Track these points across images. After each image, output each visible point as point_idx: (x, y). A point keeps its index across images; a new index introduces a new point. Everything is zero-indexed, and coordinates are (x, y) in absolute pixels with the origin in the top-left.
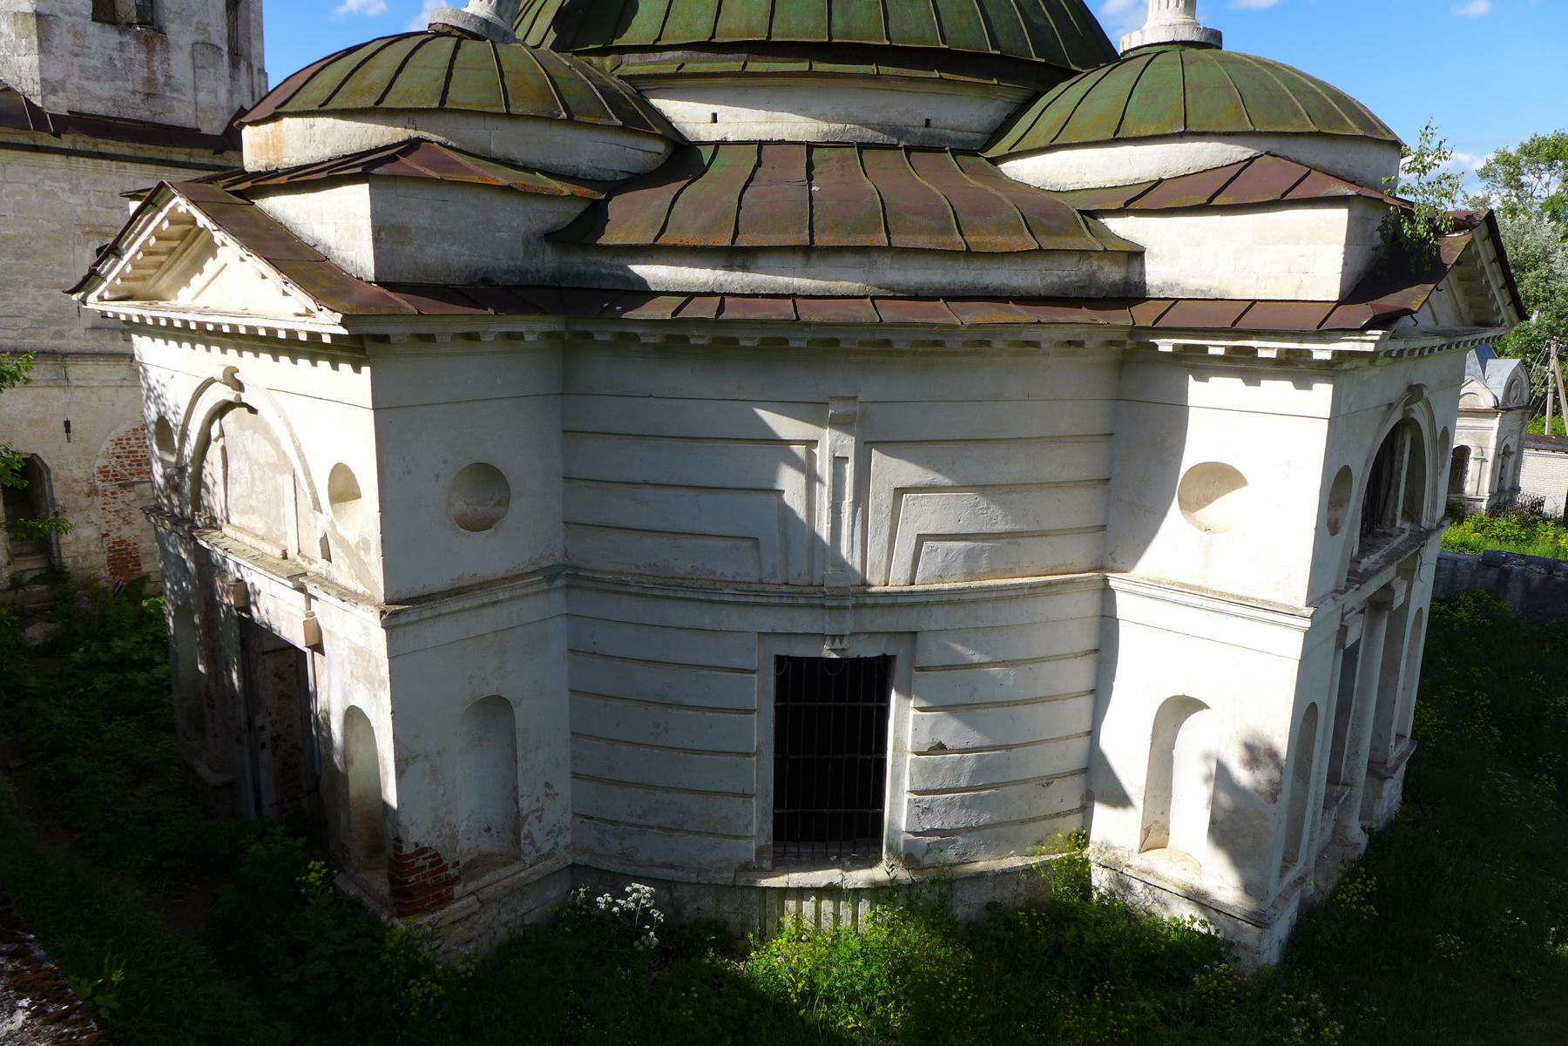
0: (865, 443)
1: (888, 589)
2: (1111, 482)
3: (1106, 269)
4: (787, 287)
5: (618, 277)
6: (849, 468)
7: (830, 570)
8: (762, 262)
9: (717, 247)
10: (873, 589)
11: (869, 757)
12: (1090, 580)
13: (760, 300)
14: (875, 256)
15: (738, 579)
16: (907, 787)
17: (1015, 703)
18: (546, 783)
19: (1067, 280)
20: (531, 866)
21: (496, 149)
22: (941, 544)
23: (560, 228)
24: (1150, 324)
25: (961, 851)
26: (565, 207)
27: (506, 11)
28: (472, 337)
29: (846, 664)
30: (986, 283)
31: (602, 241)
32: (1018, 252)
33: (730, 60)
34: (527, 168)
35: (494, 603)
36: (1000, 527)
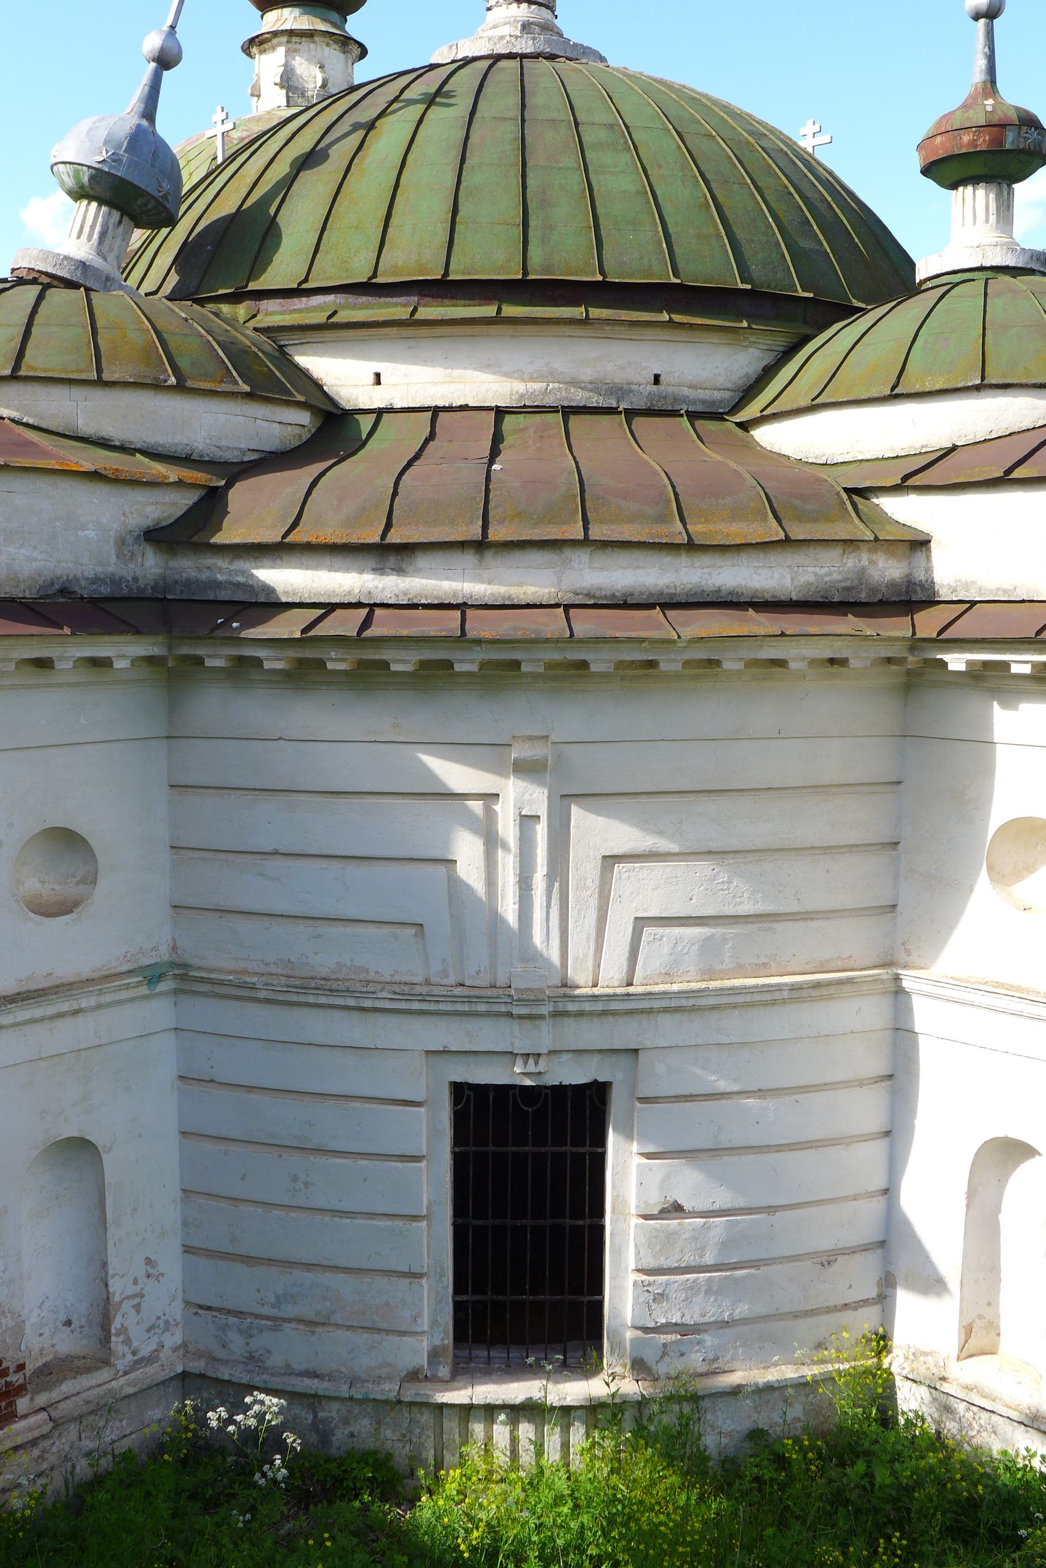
0: (562, 796)
1: (597, 991)
2: (901, 847)
3: (881, 564)
4: (455, 595)
5: (238, 585)
6: (541, 830)
7: (518, 968)
8: (422, 561)
9: (363, 544)
10: (578, 992)
11: (581, 1223)
12: (876, 980)
13: (420, 612)
14: (568, 552)
15: (397, 978)
16: (632, 1265)
17: (779, 1148)
18: (147, 1258)
19: (827, 579)
20: (126, 1373)
21: (85, 426)
22: (667, 931)
23: (164, 524)
24: (934, 635)
25: (711, 1356)
26: (172, 496)
27: (111, 250)
28: (43, 664)
29: (546, 1094)
30: (717, 585)
31: (218, 539)
32: (757, 544)
33: (396, 305)
34: (122, 448)
35: (76, 1012)
36: (747, 908)
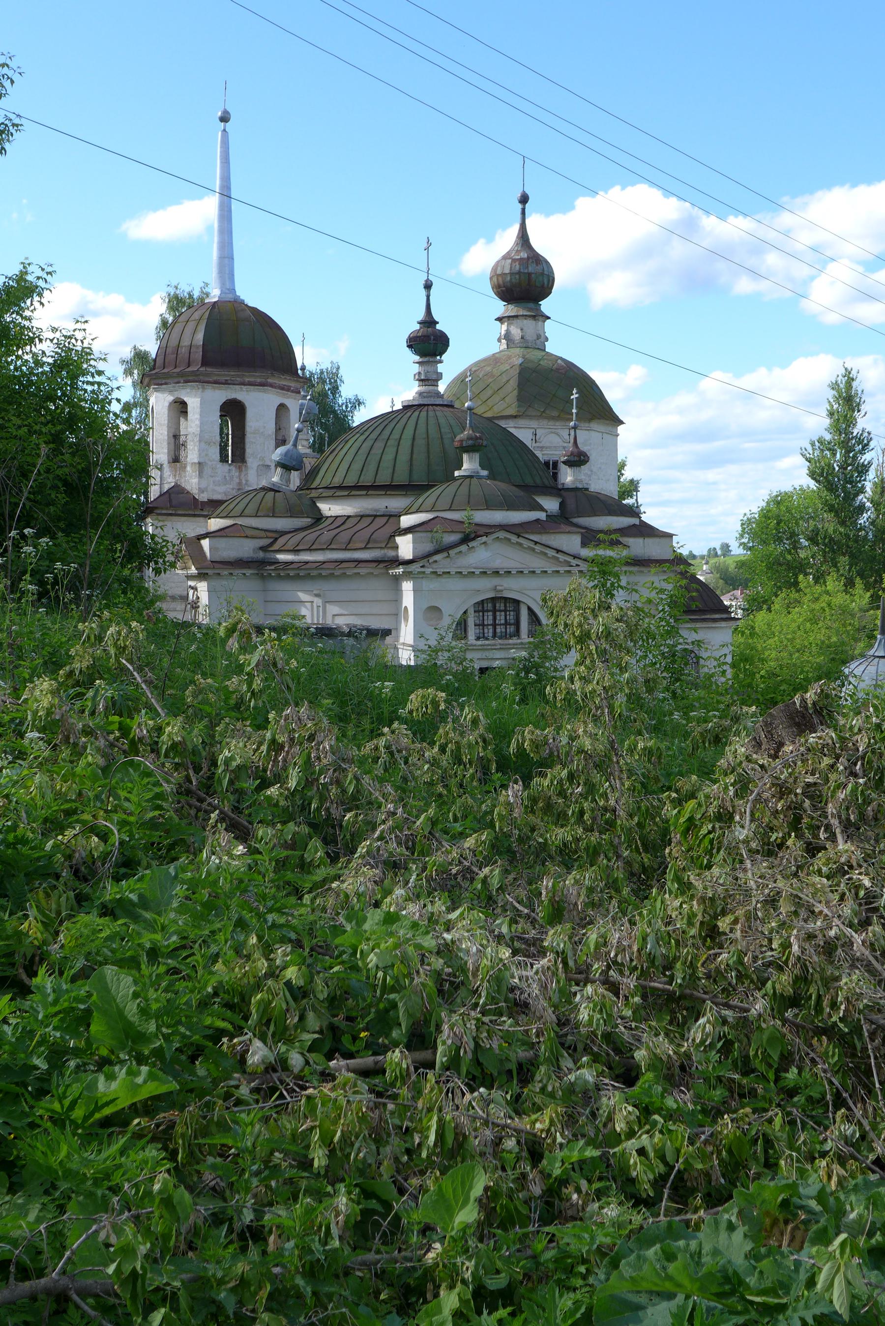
21: (254, 525)
